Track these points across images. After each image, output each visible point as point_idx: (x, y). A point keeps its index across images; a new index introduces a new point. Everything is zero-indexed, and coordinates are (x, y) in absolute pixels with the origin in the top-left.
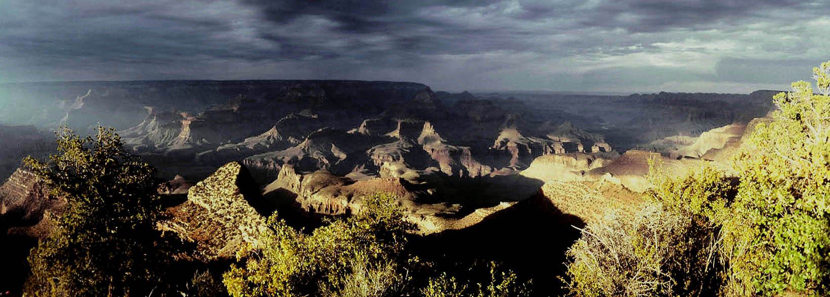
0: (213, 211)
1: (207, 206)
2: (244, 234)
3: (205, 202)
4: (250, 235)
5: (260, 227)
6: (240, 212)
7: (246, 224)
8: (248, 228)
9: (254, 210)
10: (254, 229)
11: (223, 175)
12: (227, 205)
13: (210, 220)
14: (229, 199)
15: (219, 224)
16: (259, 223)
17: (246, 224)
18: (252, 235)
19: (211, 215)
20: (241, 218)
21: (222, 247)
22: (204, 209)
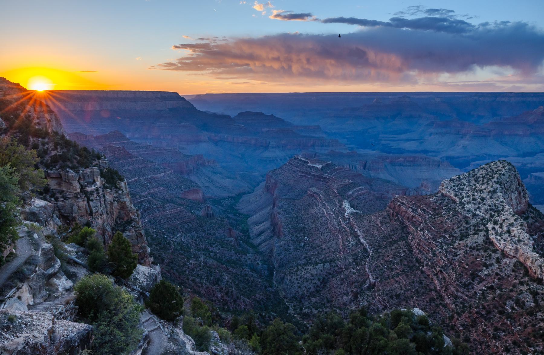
0: (461, 204)
1: (457, 200)
4: (496, 234)
6: (491, 210)
7: (496, 223)
8: (497, 227)
9: (511, 210)
10: (505, 229)
12: (479, 200)
13: (456, 213)
14: (484, 195)
15: (466, 217)
16: (512, 225)
17: (496, 223)
18: (501, 235)
19: (459, 209)
21: (460, 240)
22: (454, 202)
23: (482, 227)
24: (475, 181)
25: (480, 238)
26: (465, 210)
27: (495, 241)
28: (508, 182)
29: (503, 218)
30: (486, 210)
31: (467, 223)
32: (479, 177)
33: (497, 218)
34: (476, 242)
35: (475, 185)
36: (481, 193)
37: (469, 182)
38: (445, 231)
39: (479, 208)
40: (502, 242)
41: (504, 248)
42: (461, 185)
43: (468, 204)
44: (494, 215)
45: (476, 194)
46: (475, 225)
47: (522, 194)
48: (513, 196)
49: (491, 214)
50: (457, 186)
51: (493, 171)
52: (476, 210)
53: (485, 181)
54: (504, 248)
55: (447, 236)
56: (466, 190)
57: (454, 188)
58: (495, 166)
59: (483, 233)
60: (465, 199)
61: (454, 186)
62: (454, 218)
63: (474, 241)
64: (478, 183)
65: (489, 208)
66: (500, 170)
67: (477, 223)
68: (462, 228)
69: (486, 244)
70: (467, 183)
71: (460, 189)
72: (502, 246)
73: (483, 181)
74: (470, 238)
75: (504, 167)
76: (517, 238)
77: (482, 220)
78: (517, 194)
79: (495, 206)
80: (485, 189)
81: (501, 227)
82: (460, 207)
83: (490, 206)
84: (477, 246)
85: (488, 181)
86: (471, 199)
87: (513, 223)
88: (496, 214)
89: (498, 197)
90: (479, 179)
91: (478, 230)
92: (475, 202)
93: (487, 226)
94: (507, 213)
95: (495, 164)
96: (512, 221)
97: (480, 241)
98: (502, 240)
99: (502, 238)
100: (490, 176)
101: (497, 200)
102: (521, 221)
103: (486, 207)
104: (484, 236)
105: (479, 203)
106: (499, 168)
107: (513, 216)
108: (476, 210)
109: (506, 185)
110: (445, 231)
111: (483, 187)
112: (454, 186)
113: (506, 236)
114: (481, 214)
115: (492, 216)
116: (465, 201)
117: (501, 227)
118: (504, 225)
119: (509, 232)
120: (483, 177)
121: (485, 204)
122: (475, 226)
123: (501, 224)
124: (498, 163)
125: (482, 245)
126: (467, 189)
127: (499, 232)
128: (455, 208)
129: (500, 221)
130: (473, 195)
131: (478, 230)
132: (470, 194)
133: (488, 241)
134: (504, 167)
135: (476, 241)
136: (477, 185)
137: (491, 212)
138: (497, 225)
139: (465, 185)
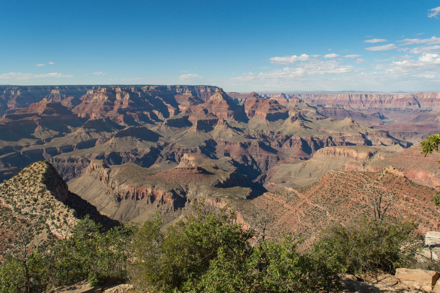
1: (10, 206)
2: (51, 228)
3: (8, 202)
4: (57, 227)
5: (67, 219)
6: (45, 207)
7: (53, 218)
8: (55, 221)
9: (62, 204)
10: (62, 221)
11: (27, 174)
12: (32, 202)
13: (14, 219)
14: (35, 196)
15: (24, 221)
16: (67, 216)
17: (53, 218)
18: (60, 227)
20: (48, 212)
22: (8, 209)
23: (42, 225)
24: (23, 184)
25: (44, 235)
26: (23, 215)
27: (57, 234)
28: (50, 179)
29: (58, 212)
30: (42, 209)
31: (28, 226)
32: (25, 180)
33: (53, 214)
34: (42, 241)
35: (23, 188)
36: (32, 195)
37: (17, 186)
38: (10, 241)
39: (34, 208)
40: (63, 232)
41: (66, 237)
42: (10, 191)
43: (23, 208)
44: (49, 211)
45: (27, 197)
46: (36, 226)
47: (63, 185)
48: (57, 190)
49: (46, 211)
50: (7, 193)
51: (35, 172)
52: (32, 211)
53: (32, 183)
54: (66, 237)
55: (13, 245)
56: (16, 195)
57: (3, 196)
58: (36, 167)
59: (45, 230)
60: (19, 204)
61: (3, 194)
62: (14, 224)
63: (40, 240)
64: (25, 186)
65: (43, 206)
66: (42, 171)
67: (37, 223)
68: (25, 231)
69: (51, 238)
70: (15, 188)
71: (9, 195)
72: (65, 236)
73: (30, 183)
74: (35, 239)
75: (43, 167)
76: (73, 226)
77: (40, 219)
78: (59, 188)
79: (48, 203)
80: (34, 190)
81: (59, 220)
82: (17, 213)
83: (43, 204)
84: (44, 244)
85: (34, 183)
86: (25, 203)
87: (67, 214)
88: (50, 210)
89: (48, 194)
90: (26, 182)
91: (40, 229)
92: (29, 204)
93: (47, 222)
94: (59, 207)
95: (35, 165)
96: (65, 212)
97: (46, 238)
98: (62, 231)
99: (62, 229)
100: (35, 177)
101: (48, 198)
102: (72, 211)
103: (39, 206)
104: (47, 232)
105: (33, 205)
106: (40, 168)
107: (65, 208)
108: (32, 211)
109: (50, 182)
110: (10, 241)
111: (32, 189)
112: (3, 194)
113: (65, 226)
114: (37, 213)
115: (48, 212)
116: (19, 206)
117: (59, 220)
118: (61, 218)
119: (65, 222)
120: (28, 179)
121: (39, 204)
122: (36, 226)
123: (58, 218)
124: (37, 164)
125: (48, 241)
126: (17, 193)
127: (58, 225)
128: (11, 215)
129: (56, 215)
130: (25, 198)
131: (40, 229)
132: (22, 198)
133: (51, 236)
134: (43, 167)
135: (42, 239)
136: (26, 188)
137: (46, 209)
138: (55, 219)
139: (13, 190)
